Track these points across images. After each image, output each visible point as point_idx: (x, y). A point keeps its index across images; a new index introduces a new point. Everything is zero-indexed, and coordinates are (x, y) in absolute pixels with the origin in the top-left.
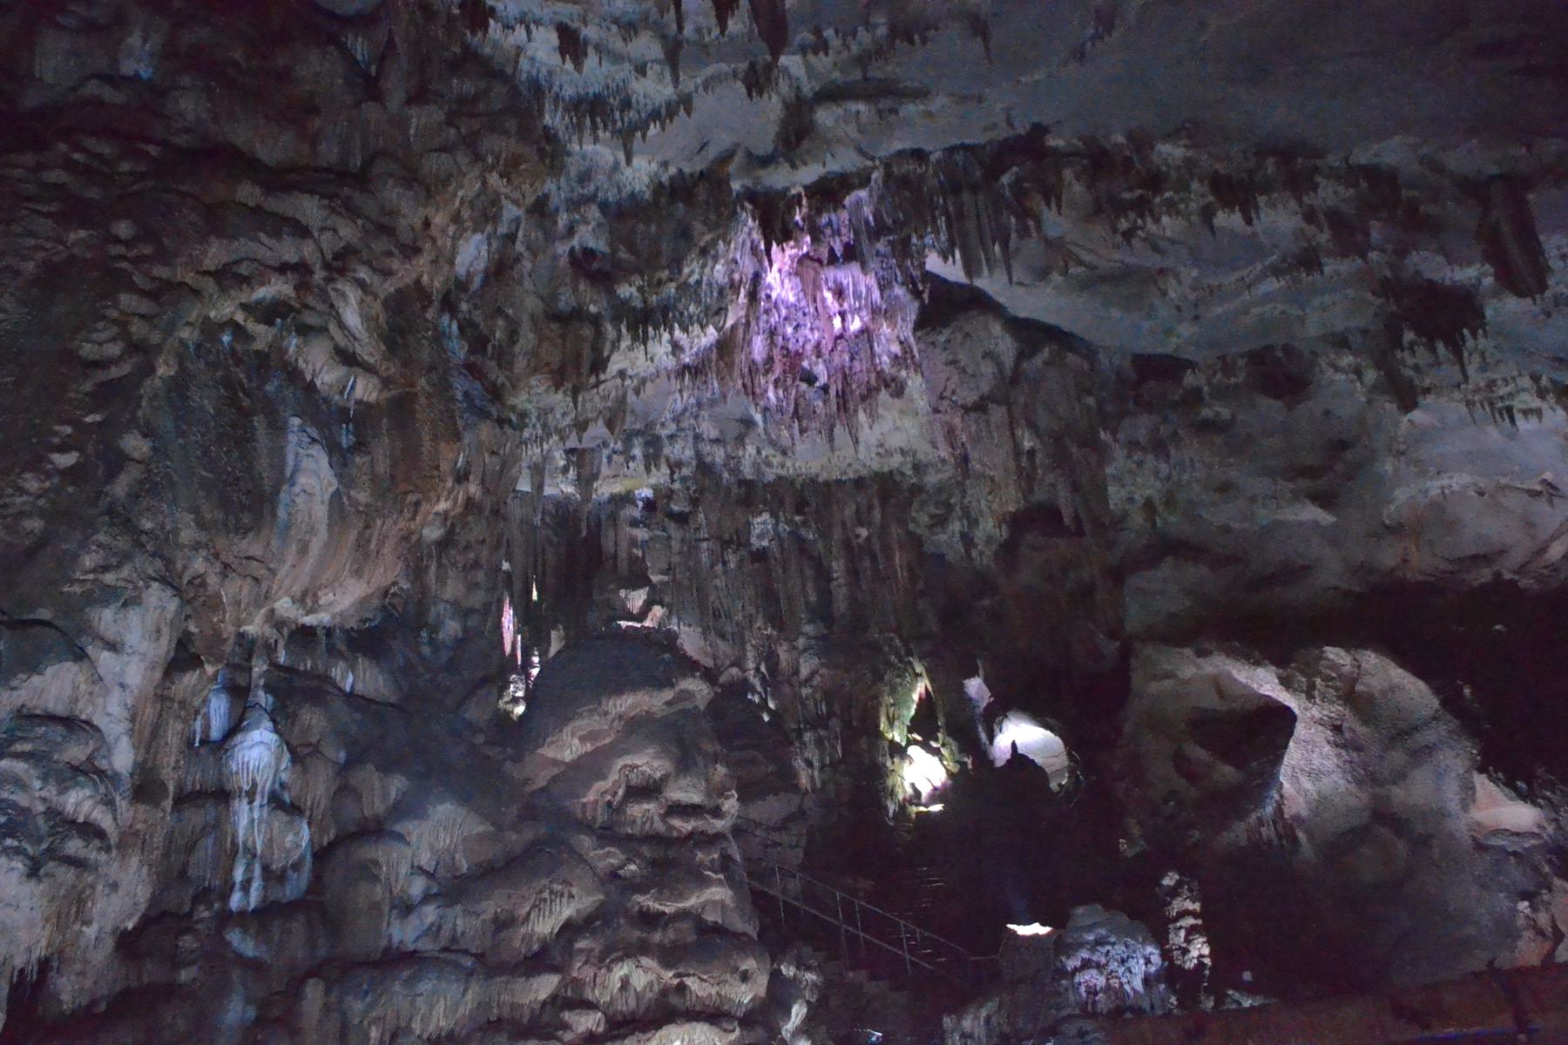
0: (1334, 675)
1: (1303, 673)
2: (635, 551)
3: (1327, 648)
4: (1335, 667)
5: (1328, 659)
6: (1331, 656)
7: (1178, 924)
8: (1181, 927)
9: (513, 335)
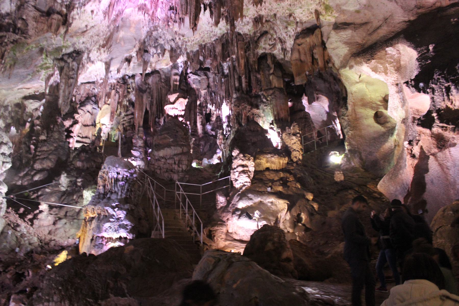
0: (392, 60)
1: (381, 64)
2: (175, 83)
3: (387, 49)
4: (392, 57)
5: (389, 54)
6: (390, 52)
7: (235, 170)
8: (237, 171)
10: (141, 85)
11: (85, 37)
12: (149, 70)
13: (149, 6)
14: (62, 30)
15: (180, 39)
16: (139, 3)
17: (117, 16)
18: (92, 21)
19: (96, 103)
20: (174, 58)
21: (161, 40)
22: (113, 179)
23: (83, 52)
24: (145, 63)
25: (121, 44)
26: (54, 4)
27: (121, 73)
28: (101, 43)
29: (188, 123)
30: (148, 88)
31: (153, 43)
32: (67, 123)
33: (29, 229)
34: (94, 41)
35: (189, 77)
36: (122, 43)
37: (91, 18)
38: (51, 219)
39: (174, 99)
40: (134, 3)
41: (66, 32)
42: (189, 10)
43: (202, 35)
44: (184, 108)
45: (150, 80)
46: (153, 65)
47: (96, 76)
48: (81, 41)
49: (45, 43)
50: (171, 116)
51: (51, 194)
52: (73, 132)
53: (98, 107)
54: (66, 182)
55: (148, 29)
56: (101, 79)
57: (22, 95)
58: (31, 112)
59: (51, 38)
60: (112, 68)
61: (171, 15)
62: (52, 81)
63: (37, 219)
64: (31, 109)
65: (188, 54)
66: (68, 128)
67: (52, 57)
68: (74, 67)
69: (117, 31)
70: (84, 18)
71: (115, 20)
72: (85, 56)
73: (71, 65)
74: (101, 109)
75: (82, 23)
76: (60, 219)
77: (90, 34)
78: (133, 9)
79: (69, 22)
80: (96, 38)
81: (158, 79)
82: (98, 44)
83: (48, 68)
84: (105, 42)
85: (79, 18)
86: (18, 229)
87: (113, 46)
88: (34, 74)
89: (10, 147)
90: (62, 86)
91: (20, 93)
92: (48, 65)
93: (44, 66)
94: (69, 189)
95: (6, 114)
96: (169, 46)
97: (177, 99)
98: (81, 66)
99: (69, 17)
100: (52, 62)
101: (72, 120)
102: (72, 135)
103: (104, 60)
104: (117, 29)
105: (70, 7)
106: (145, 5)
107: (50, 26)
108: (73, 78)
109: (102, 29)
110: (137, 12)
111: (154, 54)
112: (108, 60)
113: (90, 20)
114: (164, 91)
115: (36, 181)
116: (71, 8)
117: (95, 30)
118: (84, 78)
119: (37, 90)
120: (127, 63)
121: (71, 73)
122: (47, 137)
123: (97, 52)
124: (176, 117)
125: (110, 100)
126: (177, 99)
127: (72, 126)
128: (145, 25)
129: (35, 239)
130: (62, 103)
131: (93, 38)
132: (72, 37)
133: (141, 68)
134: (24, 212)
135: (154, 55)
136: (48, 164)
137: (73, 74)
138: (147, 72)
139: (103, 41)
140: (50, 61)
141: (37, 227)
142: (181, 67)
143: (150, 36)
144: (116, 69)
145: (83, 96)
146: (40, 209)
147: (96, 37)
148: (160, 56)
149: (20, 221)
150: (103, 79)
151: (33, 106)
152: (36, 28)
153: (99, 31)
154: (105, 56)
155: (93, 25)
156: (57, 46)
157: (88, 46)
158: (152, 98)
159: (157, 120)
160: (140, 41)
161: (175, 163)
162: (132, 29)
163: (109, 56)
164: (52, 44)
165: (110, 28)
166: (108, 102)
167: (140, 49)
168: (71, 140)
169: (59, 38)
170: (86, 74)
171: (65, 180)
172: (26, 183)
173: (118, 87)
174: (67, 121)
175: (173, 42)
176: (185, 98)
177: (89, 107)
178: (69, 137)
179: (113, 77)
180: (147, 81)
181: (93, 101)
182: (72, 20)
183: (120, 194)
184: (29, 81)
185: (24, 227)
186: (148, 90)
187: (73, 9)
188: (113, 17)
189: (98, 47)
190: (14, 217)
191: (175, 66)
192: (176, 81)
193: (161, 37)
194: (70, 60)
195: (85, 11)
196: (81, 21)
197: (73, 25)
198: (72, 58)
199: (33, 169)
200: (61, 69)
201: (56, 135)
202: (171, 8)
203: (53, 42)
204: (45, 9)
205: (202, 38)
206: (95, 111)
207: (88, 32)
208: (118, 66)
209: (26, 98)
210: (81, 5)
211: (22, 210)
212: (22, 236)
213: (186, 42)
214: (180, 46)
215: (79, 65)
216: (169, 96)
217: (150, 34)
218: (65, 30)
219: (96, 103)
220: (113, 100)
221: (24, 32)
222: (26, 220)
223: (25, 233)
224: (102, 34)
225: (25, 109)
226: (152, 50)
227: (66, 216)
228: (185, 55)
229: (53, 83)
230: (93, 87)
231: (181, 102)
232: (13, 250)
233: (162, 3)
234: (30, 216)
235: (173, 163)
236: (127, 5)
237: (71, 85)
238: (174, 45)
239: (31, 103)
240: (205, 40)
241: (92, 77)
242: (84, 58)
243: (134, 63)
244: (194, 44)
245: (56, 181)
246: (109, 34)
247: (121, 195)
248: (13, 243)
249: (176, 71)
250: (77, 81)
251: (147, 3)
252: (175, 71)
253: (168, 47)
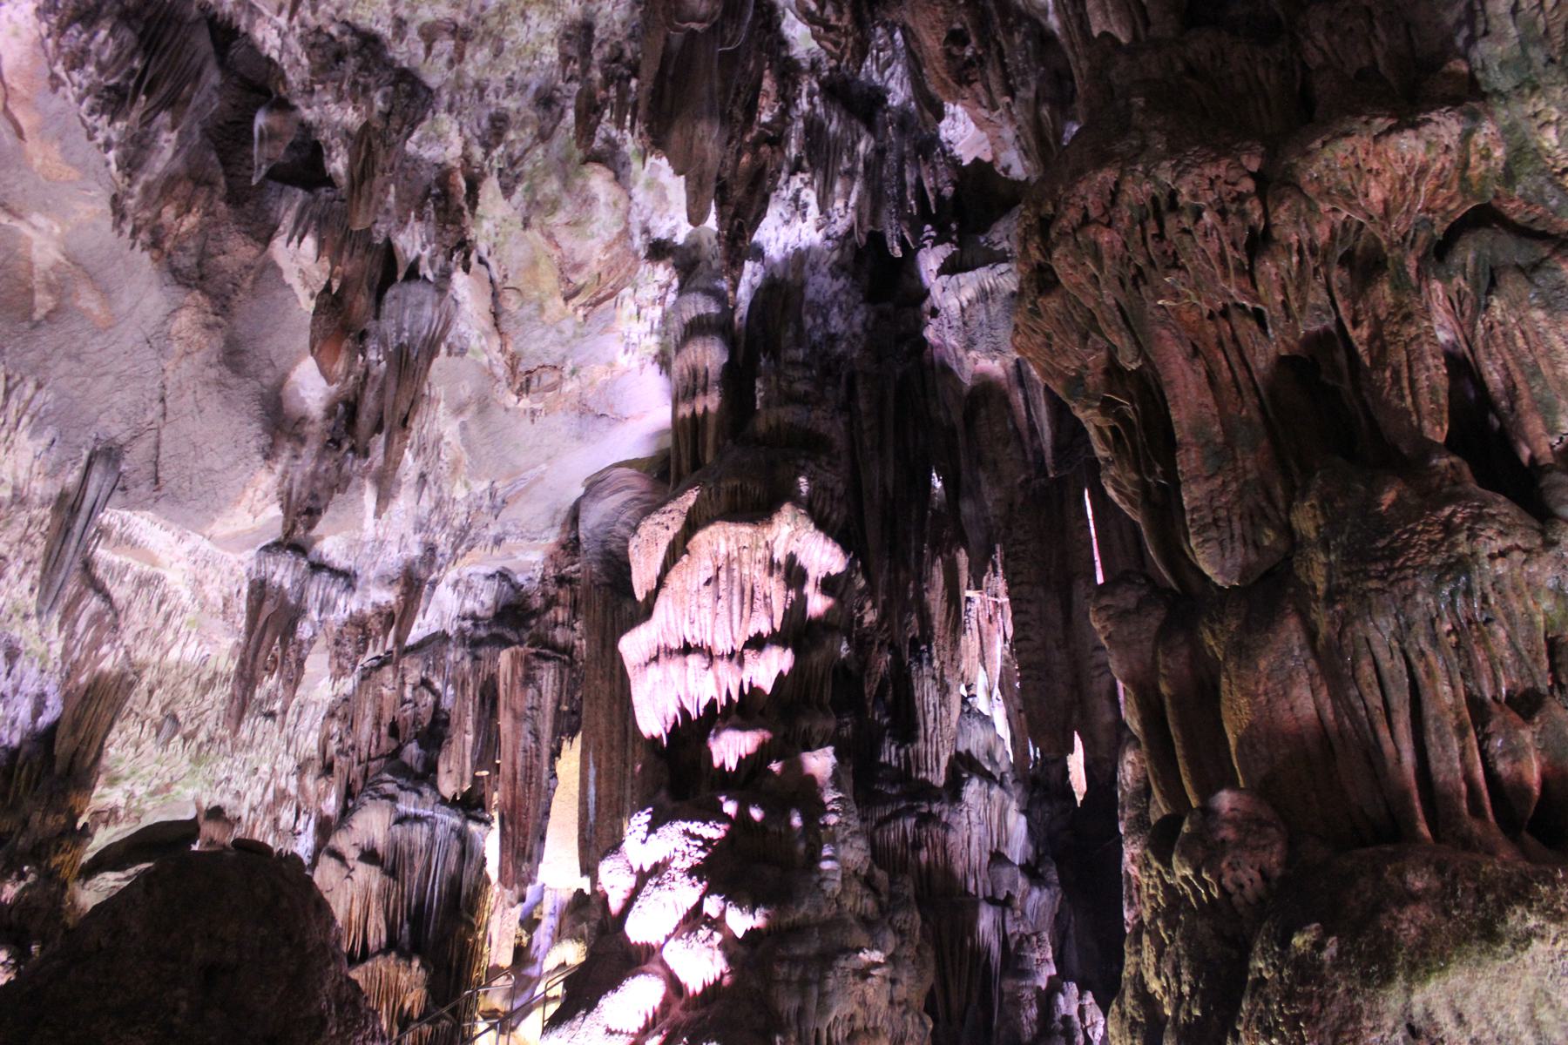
25: (84, 314)
29: (820, 762)
36: (88, 300)
97: (677, 551)
126: (677, 551)
159: (889, 754)
173: (562, 614)
176: (757, 511)
230: (414, 675)
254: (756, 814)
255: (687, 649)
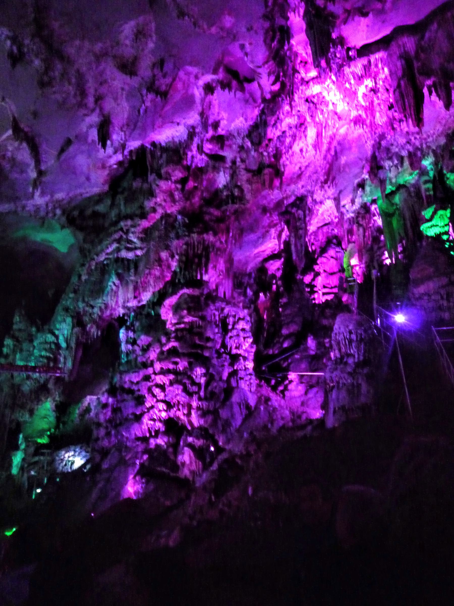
9: (241, 189)
10: (387, 209)
11: (302, 180)
12: (389, 188)
13: (364, 116)
14: (277, 183)
15: (415, 138)
16: (351, 118)
17: (330, 143)
18: (305, 160)
19: (339, 244)
20: (416, 164)
21: (394, 147)
22: (347, 341)
23: (306, 197)
24: (382, 183)
26: (262, 158)
27: (356, 204)
28: (322, 179)
30: (397, 209)
31: (385, 155)
32: (308, 279)
33: (280, 402)
34: (313, 181)
35: (448, 179)
36: (347, 170)
37: (302, 158)
38: (301, 388)
39: (431, 213)
40: (346, 120)
41: (281, 183)
42: (407, 103)
43: (444, 122)
44: (447, 221)
45: (397, 199)
46: (394, 181)
47: (329, 216)
48: (300, 186)
49: (265, 202)
50: (432, 237)
51: (301, 360)
52: (316, 286)
53: (343, 249)
54: (314, 345)
55: (373, 142)
56: (336, 218)
57: (260, 259)
58: (274, 272)
59: (269, 194)
60: (342, 203)
61: (393, 114)
62: (284, 236)
63: (288, 390)
64: (273, 270)
65: (434, 152)
66: (310, 283)
67: (276, 213)
68: (300, 217)
69: (337, 159)
70: (295, 160)
71: (329, 150)
72: (310, 199)
73: (296, 214)
74: (346, 251)
75: (294, 168)
76: (312, 387)
77: (307, 175)
78: (348, 126)
79: (281, 171)
80: (315, 177)
81: (405, 195)
82: (319, 182)
83: (275, 225)
84: (326, 177)
85: (291, 163)
86: (270, 403)
87: (337, 177)
88: (264, 236)
89: (248, 321)
90: (293, 240)
91: (258, 257)
92: (275, 222)
93: (272, 224)
94: (318, 352)
95: (252, 281)
96: (406, 152)
97: (434, 213)
98: (307, 212)
99: (280, 165)
100: (278, 217)
101: (312, 274)
102: (315, 289)
103: (332, 197)
104: (336, 157)
105: (278, 155)
106: (360, 116)
107: (264, 184)
108: (301, 229)
109: (318, 163)
110: (353, 128)
111: (390, 167)
112: (336, 195)
113: (302, 160)
114: (417, 207)
115: (286, 348)
116: (279, 156)
117: (311, 169)
118: (317, 222)
119: (273, 249)
120: (360, 189)
121: (298, 224)
122: (288, 299)
123: (321, 190)
124: (438, 237)
125: (354, 237)
126: (434, 213)
127: (313, 280)
128: (368, 139)
129: (287, 412)
130: (296, 259)
131: (312, 178)
132: (289, 185)
133: (379, 189)
134: (275, 383)
135: (392, 169)
136: (294, 328)
137: (301, 224)
138: (388, 191)
139: (324, 177)
140: (275, 218)
141: (288, 398)
142: (432, 169)
143: (379, 148)
144: (349, 201)
145: (323, 241)
146: (290, 379)
147: (315, 175)
148: (399, 167)
149: (271, 394)
150: (338, 217)
151: (274, 266)
152: (252, 190)
153: (315, 166)
154: (331, 192)
155: (307, 164)
156: (277, 200)
157: (309, 188)
158: (404, 220)
160: (367, 160)
161: (442, 298)
162: (353, 149)
163: (336, 190)
164: (273, 199)
165: (327, 160)
166: (353, 240)
167: (372, 168)
168: (316, 296)
169: (276, 191)
170: (318, 217)
171: (313, 342)
172: (277, 352)
174: (308, 276)
175: (408, 145)
176: (445, 209)
177: (332, 252)
178: (313, 292)
179: (350, 211)
180: (393, 202)
181: (334, 244)
182: (284, 168)
183: (356, 356)
184: (262, 244)
185: (275, 400)
186: (397, 212)
187: (281, 157)
188: (325, 147)
189: (320, 184)
190: (266, 391)
191: (423, 172)
192: (427, 190)
193: (392, 145)
194: (294, 210)
195: (293, 153)
196: (293, 165)
197: (286, 173)
198: (295, 207)
199: (282, 335)
200: (288, 223)
201: (297, 295)
202: (391, 107)
203: (272, 197)
204: (254, 167)
205: (445, 126)
206: (339, 255)
207: (304, 173)
208: (351, 196)
209: (267, 259)
210: (287, 148)
211: (273, 382)
212: (275, 409)
213: (425, 139)
214: (420, 147)
215: (304, 212)
216: (423, 213)
217: (377, 146)
218: (279, 181)
219: (339, 244)
220: (357, 237)
221: (241, 198)
222: (278, 392)
223: (277, 407)
224: (319, 169)
225: (267, 272)
226: (387, 164)
227: (318, 383)
228: (431, 154)
229: (286, 239)
230: (331, 228)
231: (442, 215)
232: (265, 427)
233: (379, 104)
234: (281, 388)
235: (440, 297)
236: (337, 126)
237: (301, 236)
238: (411, 149)
239: (272, 264)
240: (451, 126)
241: (326, 219)
242: (308, 202)
243: (370, 186)
244: (437, 137)
245: (303, 345)
246: (328, 166)
247: (359, 358)
248: (266, 419)
249: (425, 178)
250: (306, 231)
251: (360, 112)
252: (425, 178)
253: (404, 153)
254: (452, 244)
255: (437, 226)
